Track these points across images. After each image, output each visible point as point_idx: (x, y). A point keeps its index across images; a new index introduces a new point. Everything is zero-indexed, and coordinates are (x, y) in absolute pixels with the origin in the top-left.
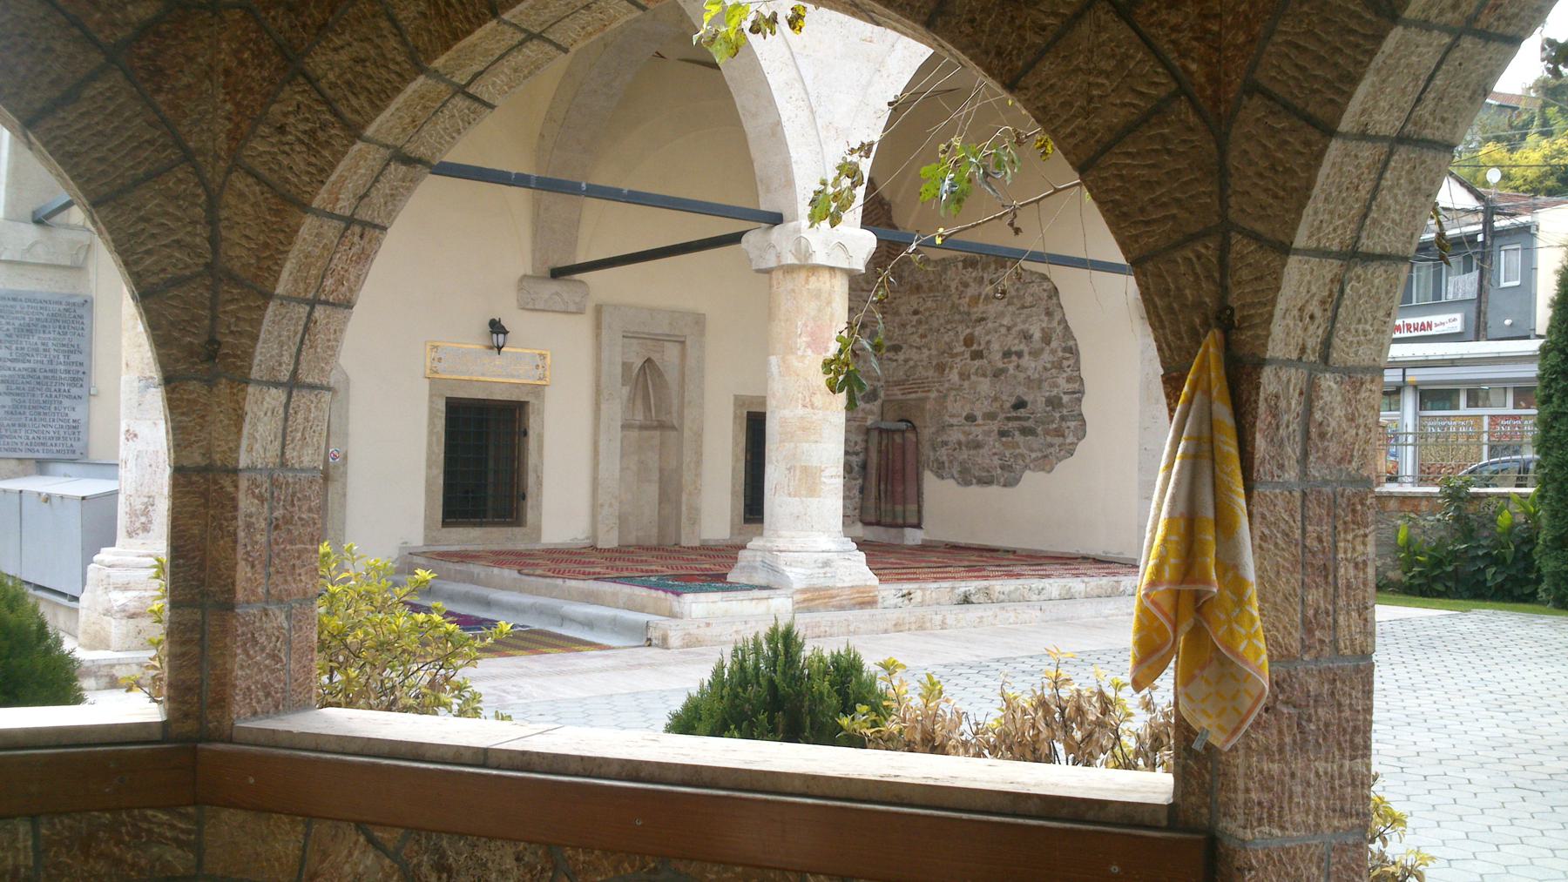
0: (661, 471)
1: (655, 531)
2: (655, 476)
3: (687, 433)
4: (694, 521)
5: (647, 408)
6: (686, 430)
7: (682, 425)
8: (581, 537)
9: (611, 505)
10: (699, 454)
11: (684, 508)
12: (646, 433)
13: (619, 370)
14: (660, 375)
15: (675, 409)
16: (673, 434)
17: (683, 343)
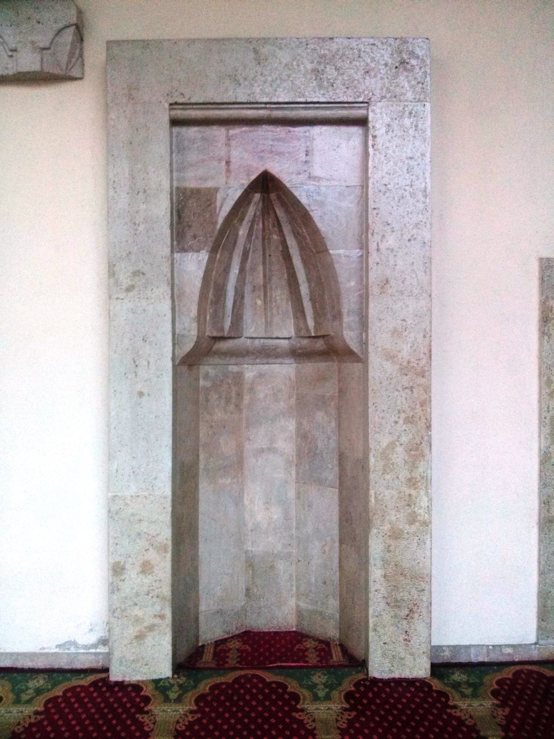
0: (341, 457)
1: (333, 605)
2: (331, 474)
3: (379, 368)
4: (411, 607)
5: (299, 311)
6: (375, 360)
7: (364, 344)
8: (92, 639)
9: (146, 568)
10: (419, 418)
11: (376, 573)
12: (310, 368)
13: (162, 208)
14: (300, 216)
15: (349, 303)
16: (358, 366)
17: (362, 122)
